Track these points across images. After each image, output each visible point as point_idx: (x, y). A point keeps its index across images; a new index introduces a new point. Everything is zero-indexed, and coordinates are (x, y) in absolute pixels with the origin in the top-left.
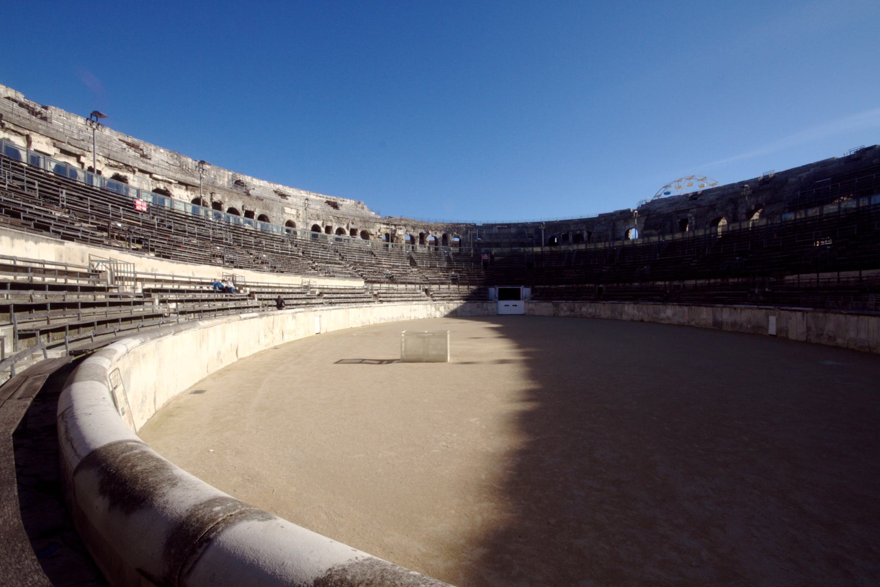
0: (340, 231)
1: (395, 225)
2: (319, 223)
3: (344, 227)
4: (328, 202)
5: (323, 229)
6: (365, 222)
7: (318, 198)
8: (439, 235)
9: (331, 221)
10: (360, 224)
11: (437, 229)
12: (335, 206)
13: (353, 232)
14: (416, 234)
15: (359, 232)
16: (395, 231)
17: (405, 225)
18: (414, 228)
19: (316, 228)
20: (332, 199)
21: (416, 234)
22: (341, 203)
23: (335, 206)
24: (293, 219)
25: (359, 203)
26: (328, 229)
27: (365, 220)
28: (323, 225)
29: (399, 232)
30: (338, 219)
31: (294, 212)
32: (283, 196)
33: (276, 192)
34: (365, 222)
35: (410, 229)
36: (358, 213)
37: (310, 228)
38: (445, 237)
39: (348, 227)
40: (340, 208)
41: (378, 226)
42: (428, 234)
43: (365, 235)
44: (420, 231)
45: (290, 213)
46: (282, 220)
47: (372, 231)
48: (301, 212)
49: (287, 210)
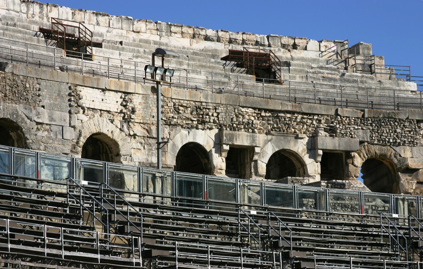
0: (284, 165)
2: (205, 138)
3: (300, 147)
4: (236, 58)
5: (219, 161)
7: (201, 45)
9: (249, 127)
10: (361, 134)
12: (263, 68)
13: (334, 165)
15: (359, 161)
19: (193, 158)
20: (252, 41)
22: (283, 55)
23: (263, 68)
24: (109, 128)
25: (354, 50)
26: (239, 160)
28: (218, 143)
30: (277, 121)
31: (113, 102)
32: (76, 45)
33: (48, 34)
34: (378, 122)
36: (349, 89)
37: (170, 160)
39: (312, 148)
40: (284, 75)
45: (99, 110)
46: (70, 134)
48: (137, 101)
49: (89, 96)
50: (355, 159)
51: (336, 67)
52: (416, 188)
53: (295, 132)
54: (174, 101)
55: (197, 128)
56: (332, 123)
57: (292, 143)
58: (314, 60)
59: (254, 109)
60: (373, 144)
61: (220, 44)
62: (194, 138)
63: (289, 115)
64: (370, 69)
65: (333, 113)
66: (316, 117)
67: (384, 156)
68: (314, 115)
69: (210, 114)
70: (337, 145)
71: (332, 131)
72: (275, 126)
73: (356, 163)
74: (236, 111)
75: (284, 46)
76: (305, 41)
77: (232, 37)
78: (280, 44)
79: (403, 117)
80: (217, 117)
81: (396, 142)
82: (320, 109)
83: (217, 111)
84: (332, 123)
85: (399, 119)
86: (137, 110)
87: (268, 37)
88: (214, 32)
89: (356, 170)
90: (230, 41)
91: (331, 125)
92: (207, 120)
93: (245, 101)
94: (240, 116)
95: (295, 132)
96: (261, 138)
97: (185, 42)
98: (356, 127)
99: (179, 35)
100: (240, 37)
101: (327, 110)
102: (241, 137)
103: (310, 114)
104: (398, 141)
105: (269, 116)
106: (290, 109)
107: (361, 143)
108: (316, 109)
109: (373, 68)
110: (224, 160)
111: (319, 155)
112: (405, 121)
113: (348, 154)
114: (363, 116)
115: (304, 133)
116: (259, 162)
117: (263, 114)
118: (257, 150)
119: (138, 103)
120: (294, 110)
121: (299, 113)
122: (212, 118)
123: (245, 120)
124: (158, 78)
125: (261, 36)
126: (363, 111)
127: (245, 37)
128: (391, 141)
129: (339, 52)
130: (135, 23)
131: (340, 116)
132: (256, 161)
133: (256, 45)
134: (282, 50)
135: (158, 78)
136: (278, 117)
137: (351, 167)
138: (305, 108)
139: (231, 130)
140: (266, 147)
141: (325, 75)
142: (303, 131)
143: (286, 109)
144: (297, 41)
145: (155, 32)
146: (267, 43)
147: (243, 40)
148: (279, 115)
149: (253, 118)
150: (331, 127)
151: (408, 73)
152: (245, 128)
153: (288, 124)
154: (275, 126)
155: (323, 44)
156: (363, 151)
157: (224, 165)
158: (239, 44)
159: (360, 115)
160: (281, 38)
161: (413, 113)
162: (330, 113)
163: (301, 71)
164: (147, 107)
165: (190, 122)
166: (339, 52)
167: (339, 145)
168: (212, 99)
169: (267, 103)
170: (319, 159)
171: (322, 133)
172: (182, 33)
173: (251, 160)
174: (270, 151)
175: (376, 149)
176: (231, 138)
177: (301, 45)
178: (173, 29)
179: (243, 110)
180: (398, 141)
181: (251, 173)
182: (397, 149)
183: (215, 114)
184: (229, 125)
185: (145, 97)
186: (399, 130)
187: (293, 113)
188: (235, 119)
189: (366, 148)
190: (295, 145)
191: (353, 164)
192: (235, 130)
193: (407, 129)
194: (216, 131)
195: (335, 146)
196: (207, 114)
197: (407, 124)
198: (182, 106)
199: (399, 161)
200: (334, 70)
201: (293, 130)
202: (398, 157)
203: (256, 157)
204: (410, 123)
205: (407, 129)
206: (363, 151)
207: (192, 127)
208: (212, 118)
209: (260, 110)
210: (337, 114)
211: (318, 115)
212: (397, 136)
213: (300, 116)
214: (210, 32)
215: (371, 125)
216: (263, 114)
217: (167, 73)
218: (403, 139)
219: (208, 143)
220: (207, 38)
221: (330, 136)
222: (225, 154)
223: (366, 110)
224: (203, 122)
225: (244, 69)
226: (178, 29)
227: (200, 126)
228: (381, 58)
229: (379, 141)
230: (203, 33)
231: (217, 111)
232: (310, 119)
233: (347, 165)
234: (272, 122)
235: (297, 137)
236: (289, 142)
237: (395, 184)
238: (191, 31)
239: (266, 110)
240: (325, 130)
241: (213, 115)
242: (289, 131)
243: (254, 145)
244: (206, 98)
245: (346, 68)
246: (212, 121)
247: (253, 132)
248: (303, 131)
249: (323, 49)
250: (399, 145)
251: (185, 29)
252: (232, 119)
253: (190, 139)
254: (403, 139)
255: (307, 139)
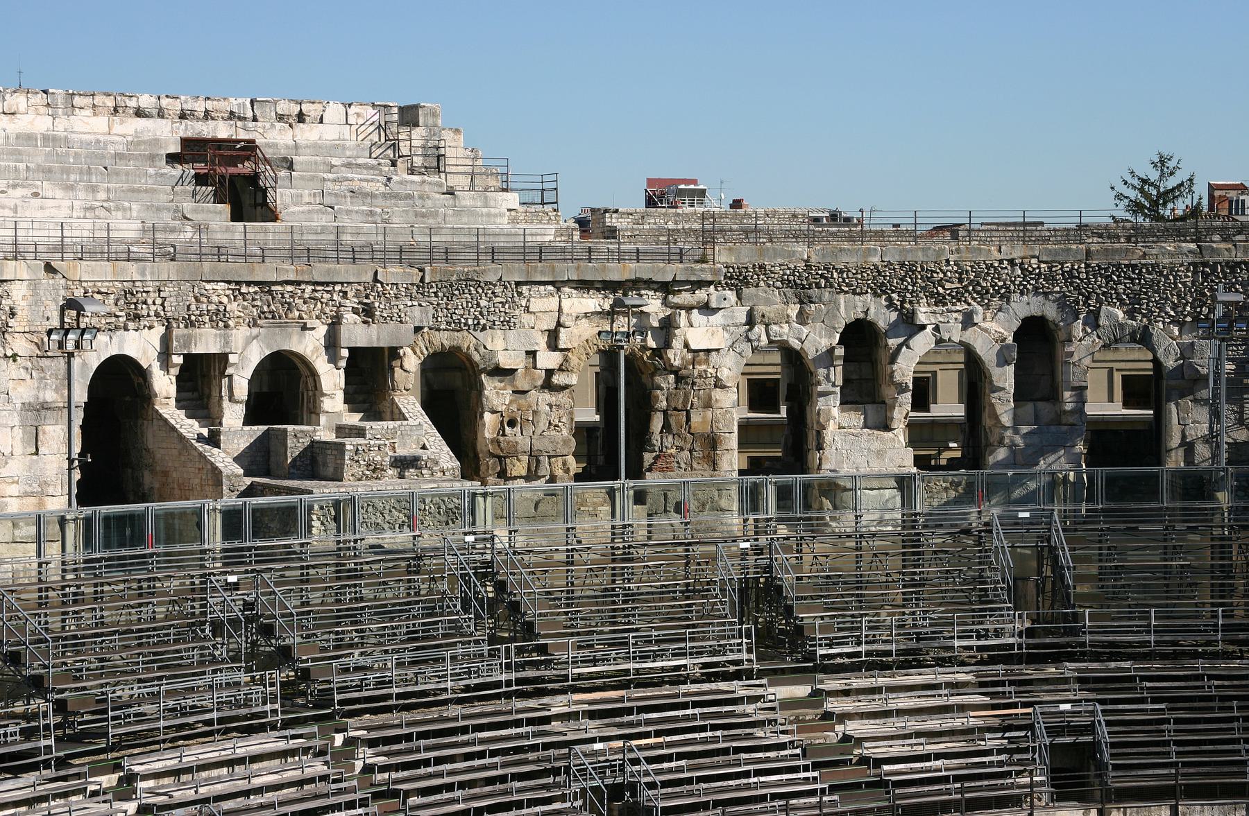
0: (282, 390)
1: (666, 288)
2: (141, 345)
3: (310, 345)
5: (164, 385)
6: (449, 289)
8: (992, 331)
9: (220, 318)
10: (418, 314)
11: (981, 286)
13: (369, 376)
14: (817, 339)
15: (412, 362)
16: (667, 327)
17: (738, 281)
18: (803, 288)
21: (817, 339)
25: (409, 116)
27: (463, 276)
28: (165, 356)
29: (698, 332)
35: (772, 301)
38: (1036, 341)
39: (332, 344)
40: (281, 197)
41: (543, 303)
42: (909, 325)
43: (453, 393)
44: (848, 308)
47: (503, 347)
50: (405, 359)
51: (375, 162)
52: (511, 402)
53: (300, 317)
54: (84, 284)
55: (126, 329)
56: (367, 297)
57: (295, 338)
58: (336, 148)
59: (229, 282)
60: (438, 330)
61: (164, 121)
62: (121, 347)
63: (290, 288)
64: (436, 162)
65: (369, 278)
66: (338, 288)
67: (455, 350)
68: (335, 283)
69: (150, 301)
70: (375, 338)
71: (367, 312)
72: (266, 309)
73: (406, 366)
74: (196, 290)
75: (281, 118)
76: (319, 107)
77: (185, 107)
78: (273, 114)
79: (493, 278)
80: (162, 305)
81: (478, 323)
82: (345, 271)
83: (162, 294)
84: (367, 297)
85: (486, 283)
86: (18, 311)
87: (252, 102)
88: (154, 100)
89: (407, 378)
90: (183, 116)
91: (366, 301)
92: (145, 313)
93: (212, 272)
94: (205, 300)
95: (300, 317)
96: (240, 334)
97: (100, 124)
98: (409, 303)
99: (88, 112)
100: (200, 107)
101: (359, 274)
102: (203, 339)
103: (328, 284)
104: (483, 322)
105: (256, 293)
106: (292, 277)
107: (418, 329)
108: (339, 273)
109: (442, 163)
110: (174, 379)
111: (343, 358)
112: (495, 285)
113: (394, 353)
114: (422, 280)
115: (318, 317)
116: (235, 378)
117: (244, 289)
118: (232, 359)
119: (20, 298)
120: (300, 278)
121: (307, 283)
122: (153, 308)
123: (212, 307)
124: (70, 346)
125: (240, 100)
126: (422, 270)
127: (210, 105)
128: (470, 322)
129: (383, 124)
130: (7, 97)
131: (382, 283)
132: (230, 377)
133: (230, 119)
134: (279, 125)
135: (70, 346)
136: (270, 292)
137: (398, 371)
138: (319, 271)
139: (186, 327)
140: (248, 350)
141: (356, 185)
142: (314, 314)
143: (286, 278)
144: (305, 108)
145: (43, 110)
146: (249, 114)
147: (206, 111)
148: (273, 288)
149: (225, 300)
150: (365, 304)
151: (504, 170)
152: (211, 320)
153: (289, 304)
154: (266, 309)
155: (352, 110)
156: (421, 343)
157: (172, 390)
158: (198, 119)
159: (417, 280)
160: (275, 103)
161: (509, 271)
162: (363, 280)
163: (312, 179)
164: (36, 301)
165: (113, 319)
166: (383, 124)
167: (378, 338)
168: (152, 273)
169: (252, 271)
170: (343, 364)
171: (349, 317)
172: (94, 106)
173: (222, 374)
174: (256, 355)
175: (444, 339)
176: (188, 340)
177: (312, 114)
178: (78, 101)
179: (208, 286)
180: (483, 322)
181: (221, 397)
182: (478, 334)
183: (159, 301)
184: (184, 318)
185: (34, 285)
186: (483, 303)
187: (298, 283)
188: (193, 307)
189: (426, 337)
190: (300, 342)
191: (401, 367)
192: (193, 325)
193: (499, 300)
194: (160, 330)
195: (370, 339)
196: (145, 303)
197: (498, 290)
198: (99, 292)
199: (483, 357)
200: (372, 168)
201: (297, 314)
202: (482, 350)
203: (229, 371)
204: (506, 288)
205: (499, 300)
206: (421, 343)
207: (117, 328)
208: (153, 308)
209: (237, 283)
210: (376, 280)
211: (342, 283)
212: (481, 313)
213: (310, 287)
214: (146, 101)
215: (436, 296)
216: (244, 289)
217: (86, 336)
218: (491, 318)
219: (145, 352)
220: (139, 113)
221: (365, 322)
222: (175, 371)
223: (428, 269)
224: (138, 317)
225: (210, 188)
226: (88, 100)
227: (131, 325)
228: (457, 131)
229: (448, 323)
230: (132, 103)
231: (162, 294)
232: (327, 292)
233: (392, 369)
234: (259, 303)
235: (304, 328)
236: (290, 336)
237: (474, 393)
238: (110, 103)
239: (249, 284)
240: (355, 311)
241: (154, 303)
242: (290, 316)
243: (228, 350)
244: (143, 274)
245: (394, 164)
246: (152, 313)
247: (227, 326)
248: (314, 314)
249: (352, 120)
250: (484, 328)
251: (99, 100)
252: (188, 307)
253: (114, 351)
254: (491, 318)
255: (322, 330)
